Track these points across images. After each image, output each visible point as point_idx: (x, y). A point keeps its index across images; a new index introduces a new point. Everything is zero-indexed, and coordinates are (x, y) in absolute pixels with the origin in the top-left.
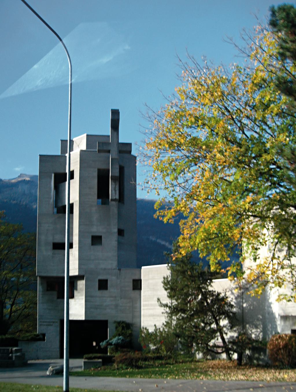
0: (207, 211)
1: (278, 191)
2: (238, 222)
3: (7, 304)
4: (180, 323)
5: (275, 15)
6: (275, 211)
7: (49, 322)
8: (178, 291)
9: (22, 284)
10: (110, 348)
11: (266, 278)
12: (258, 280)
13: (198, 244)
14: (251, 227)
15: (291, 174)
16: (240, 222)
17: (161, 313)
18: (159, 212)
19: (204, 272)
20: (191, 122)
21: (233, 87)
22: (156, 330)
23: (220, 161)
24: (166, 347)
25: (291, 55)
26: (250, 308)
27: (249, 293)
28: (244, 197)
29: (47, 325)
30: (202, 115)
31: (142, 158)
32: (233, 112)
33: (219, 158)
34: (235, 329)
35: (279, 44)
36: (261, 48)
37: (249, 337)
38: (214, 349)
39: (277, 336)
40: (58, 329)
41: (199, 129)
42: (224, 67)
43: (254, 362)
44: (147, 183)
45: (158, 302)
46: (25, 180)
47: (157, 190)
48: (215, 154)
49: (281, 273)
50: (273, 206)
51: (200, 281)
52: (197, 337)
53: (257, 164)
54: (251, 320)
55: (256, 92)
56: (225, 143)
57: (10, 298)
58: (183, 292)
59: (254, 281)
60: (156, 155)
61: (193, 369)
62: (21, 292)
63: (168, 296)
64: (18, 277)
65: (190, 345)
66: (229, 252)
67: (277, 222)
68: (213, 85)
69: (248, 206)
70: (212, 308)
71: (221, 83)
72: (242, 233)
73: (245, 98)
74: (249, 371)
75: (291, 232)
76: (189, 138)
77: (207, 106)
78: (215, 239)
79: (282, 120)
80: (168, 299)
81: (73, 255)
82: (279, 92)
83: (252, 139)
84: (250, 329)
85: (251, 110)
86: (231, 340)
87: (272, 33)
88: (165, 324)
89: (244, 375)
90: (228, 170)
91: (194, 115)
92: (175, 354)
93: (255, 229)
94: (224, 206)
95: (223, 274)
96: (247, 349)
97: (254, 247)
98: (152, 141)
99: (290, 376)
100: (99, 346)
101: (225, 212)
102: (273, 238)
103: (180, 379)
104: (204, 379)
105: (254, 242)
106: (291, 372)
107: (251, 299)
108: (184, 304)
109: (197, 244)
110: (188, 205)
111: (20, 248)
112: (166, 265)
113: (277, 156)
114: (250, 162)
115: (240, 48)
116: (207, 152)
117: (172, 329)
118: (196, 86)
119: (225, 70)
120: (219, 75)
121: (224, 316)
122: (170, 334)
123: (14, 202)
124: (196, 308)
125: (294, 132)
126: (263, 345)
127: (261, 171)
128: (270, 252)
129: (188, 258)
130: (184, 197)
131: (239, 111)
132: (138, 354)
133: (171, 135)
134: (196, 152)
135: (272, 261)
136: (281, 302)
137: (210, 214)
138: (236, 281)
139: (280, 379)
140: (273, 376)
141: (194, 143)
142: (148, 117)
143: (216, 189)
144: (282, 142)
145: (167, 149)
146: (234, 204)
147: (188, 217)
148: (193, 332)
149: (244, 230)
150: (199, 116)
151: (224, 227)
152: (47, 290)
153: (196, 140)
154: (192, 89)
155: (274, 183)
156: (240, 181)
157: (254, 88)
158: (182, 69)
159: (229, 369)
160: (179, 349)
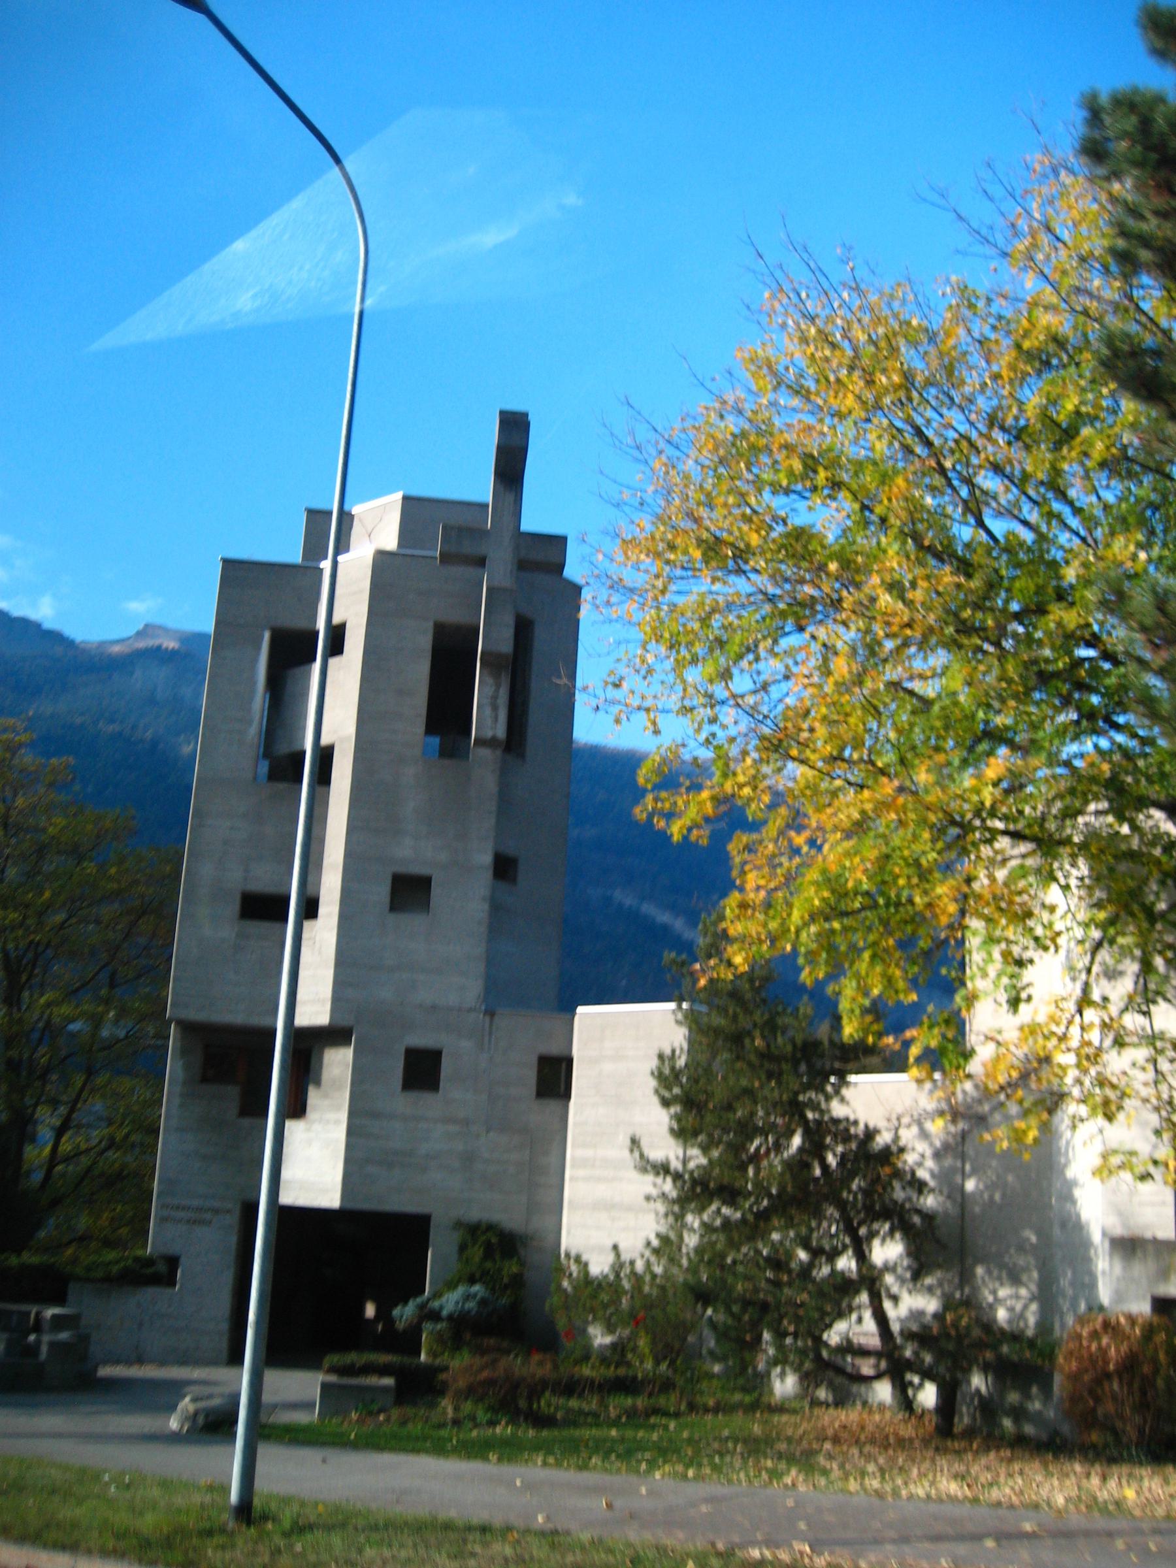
0: (836, 803)
1: (1104, 743)
2: (953, 855)
3: (40, 1127)
4: (716, 1243)
5: (1101, 121)
6: (1093, 819)
7: (200, 1209)
8: (712, 1111)
9: (109, 1047)
10: (431, 1333)
11: (1055, 1081)
12: (1026, 1086)
13: (798, 932)
14: (1001, 874)
15: (1155, 686)
16: (959, 855)
18: (656, 800)
19: (817, 1044)
20: (791, 473)
22: (618, 1267)
23: (891, 619)
24: (654, 1342)
25: (1156, 260)
26: (991, 1197)
27: (987, 1137)
28: (977, 761)
29: (188, 1221)
30: (830, 450)
31: (604, 594)
32: (942, 447)
33: (889, 611)
34: (928, 1281)
35: (1113, 220)
36: (1049, 229)
37: (985, 1320)
38: (844, 1360)
39: (1096, 1319)
40: (233, 1240)
41: (819, 501)
42: (915, 289)
43: (1001, 1426)
44: (617, 686)
45: (632, 1151)
46: (159, 648)
47: (652, 715)
48: (873, 594)
49: (1116, 1063)
50: (1086, 802)
51: (800, 1076)
52: (778, 1305)
53: (1029, 640)
54: (994, 1249)
55: (1028, 379)
56: (913, 557)
57: (54, 1103)
58: (731, 1116)
59: (1009, 1091)
60: (654, 586)
61: (756, 1440)
62: (100, 1080)
63: (672, 1131)
64: (97, 1022)
65: (748, 1338)
66: (916, 969)
67: (1101, 861)
68: (872, 349)
69: (992, 794)
70: (841, 1189)
71: (902, 342)
72: (965, 897)
74: (983, 1461)
75: (1153, 904)
76: (780, 529)
77: (849, 422)
78: (863, 914)
79: (1120, 487)
81: (317, 945)
82: (1113, 386)
83: (1011, 547)
84: (991, 1286)
85: (1009, 443)
86: (915, 1327)
87: (1091, 180)
88: (655, 1243)
89: (963, 1478)
91: (800, 449)
92: (689, 1374)
93: (1016, 884)
94: (901, 789)
95: (887, 1053)
96: (975, 1369)
98: (644, 534)
99: (1147, 1494)
100: (390, 1322)
101: (905, 813)
102: (1086, 925)
103: (703, 1479)
104: (802, 1488)
105: (1010, 934)
106: (1151, 1478)
107: (994, 1163)
109: (793, 929)
110: (765, 777)
111: (116, 905)
112: (672, 1005)
113: (1104, 615)
114: (1002, 631)
115: (975, 225)
116: (843, 585)
117: (680, 1266)
118: (812, 348)
119: (920, 299)
120: (898, 313)
121: (887, 1226)
122: (674, 1285)
123: (112, 728)
124: (780, 1184)
125: (1166, 531)
126: (1041, 1354)
127: (1043, 665)
128: (1074, 979)
129: (757, 984)
131: (964, 444)
132: (541, 1363)
133: (714, 515)
134: (802, 581)
135: (1080, 1012)
136: (1113, 1179)
137: (848, 817)
138: (939, 1083)
139: (1105, 1502)
140: (1079, 1488)
141: (799, 548)
142: (633, 444)
143: (874, 726)
144: (1121, 564)
145: (697, 566)
146: (937, 783)
147: (765, 822)
148: (763, 1284)
149: (976, 886)
150: (819, 454)
151: (897, 870)
152: (205, 1079)
153: (805, 537)
154: (797, 355)
155: (1090, 715)
156: (962, 698)
157: (1022, 366)
158: (765, 283)
159: (903, 1448)
160: (704, 1352)
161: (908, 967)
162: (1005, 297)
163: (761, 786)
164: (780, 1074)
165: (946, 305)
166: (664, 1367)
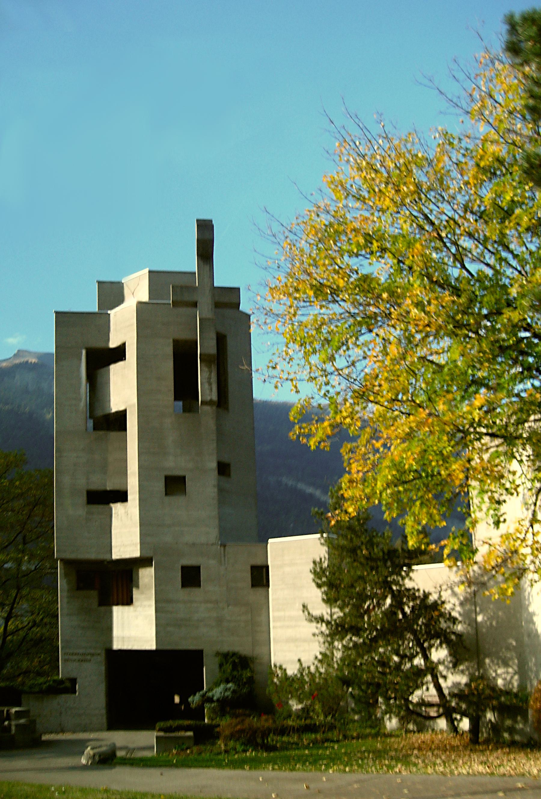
0: (396, 424)
2: (460, 448)
4: (351, 655)
8: (343, 589)
11: (521, 562)
13: (381, 493)
14: (486, 457)
16: (463, 448)
17: (311, 635)
19: (395, 551)
21: (439, 175)
23: (418, 322)
24: (323, 706)
32: (440, 225)
33: (417, 318)
42: (419, 136)
56: (428, 288)
58: (353, 590)
63: (323, 600)
65: (371, 701)
66: (444, 509)
71: (414, 167)
72: (468, 469)
73: (464, 196)
78: (414, 482)
80: (324, 605)
88: (320, 657)
90: (436, 341)
92: (342, 721)
93: (494, 461)
94: (430, 414)
97: (493, 497)
101: (433, 427)
102: (533, 481)
103: (354, 771)
105: (493, 488)
108: (356, 617)
109: (378, 492)
110: (357, 412)
112: (318, 535)
116: (391, 305)
117: (333, 668)
119: (422, 141)
120: (411, 150)
122: (331, 678)
124: (381, 624)
128: (527, 509)
130: (348, 397)
131: (452, 222)
137: (403, 431)
143: (414, 382)
146: (449, 410)
147: (359, 436)
148: (377, 674)
149: (473, 463)
151: (431, 458)
160: (349, 709)
161: (440, 508)
162: (469, 137)
163: (355, 417)
164: (377, 567)
165: (437, 144)
166: (329, 718)
